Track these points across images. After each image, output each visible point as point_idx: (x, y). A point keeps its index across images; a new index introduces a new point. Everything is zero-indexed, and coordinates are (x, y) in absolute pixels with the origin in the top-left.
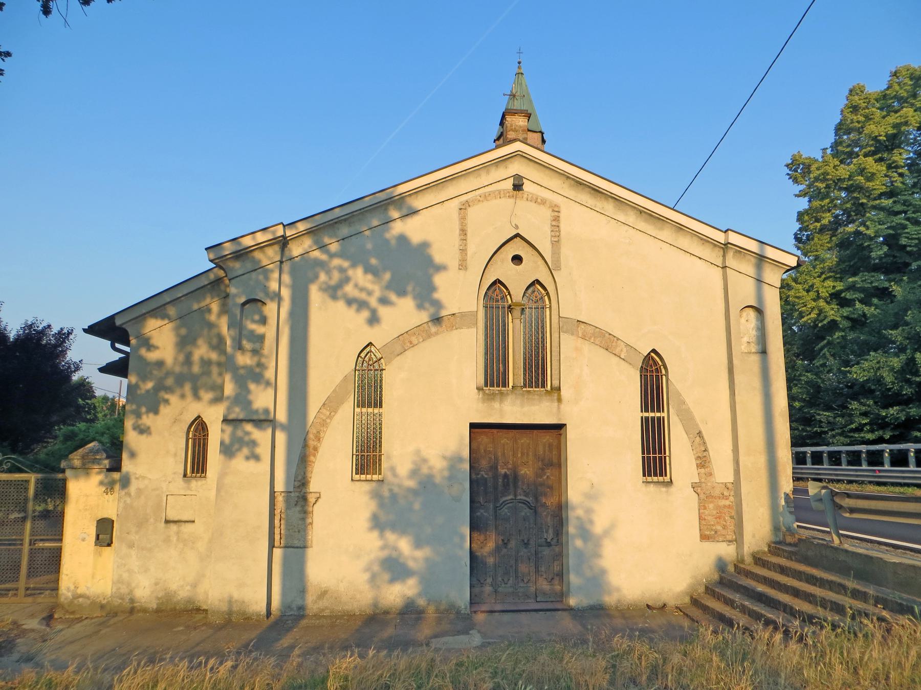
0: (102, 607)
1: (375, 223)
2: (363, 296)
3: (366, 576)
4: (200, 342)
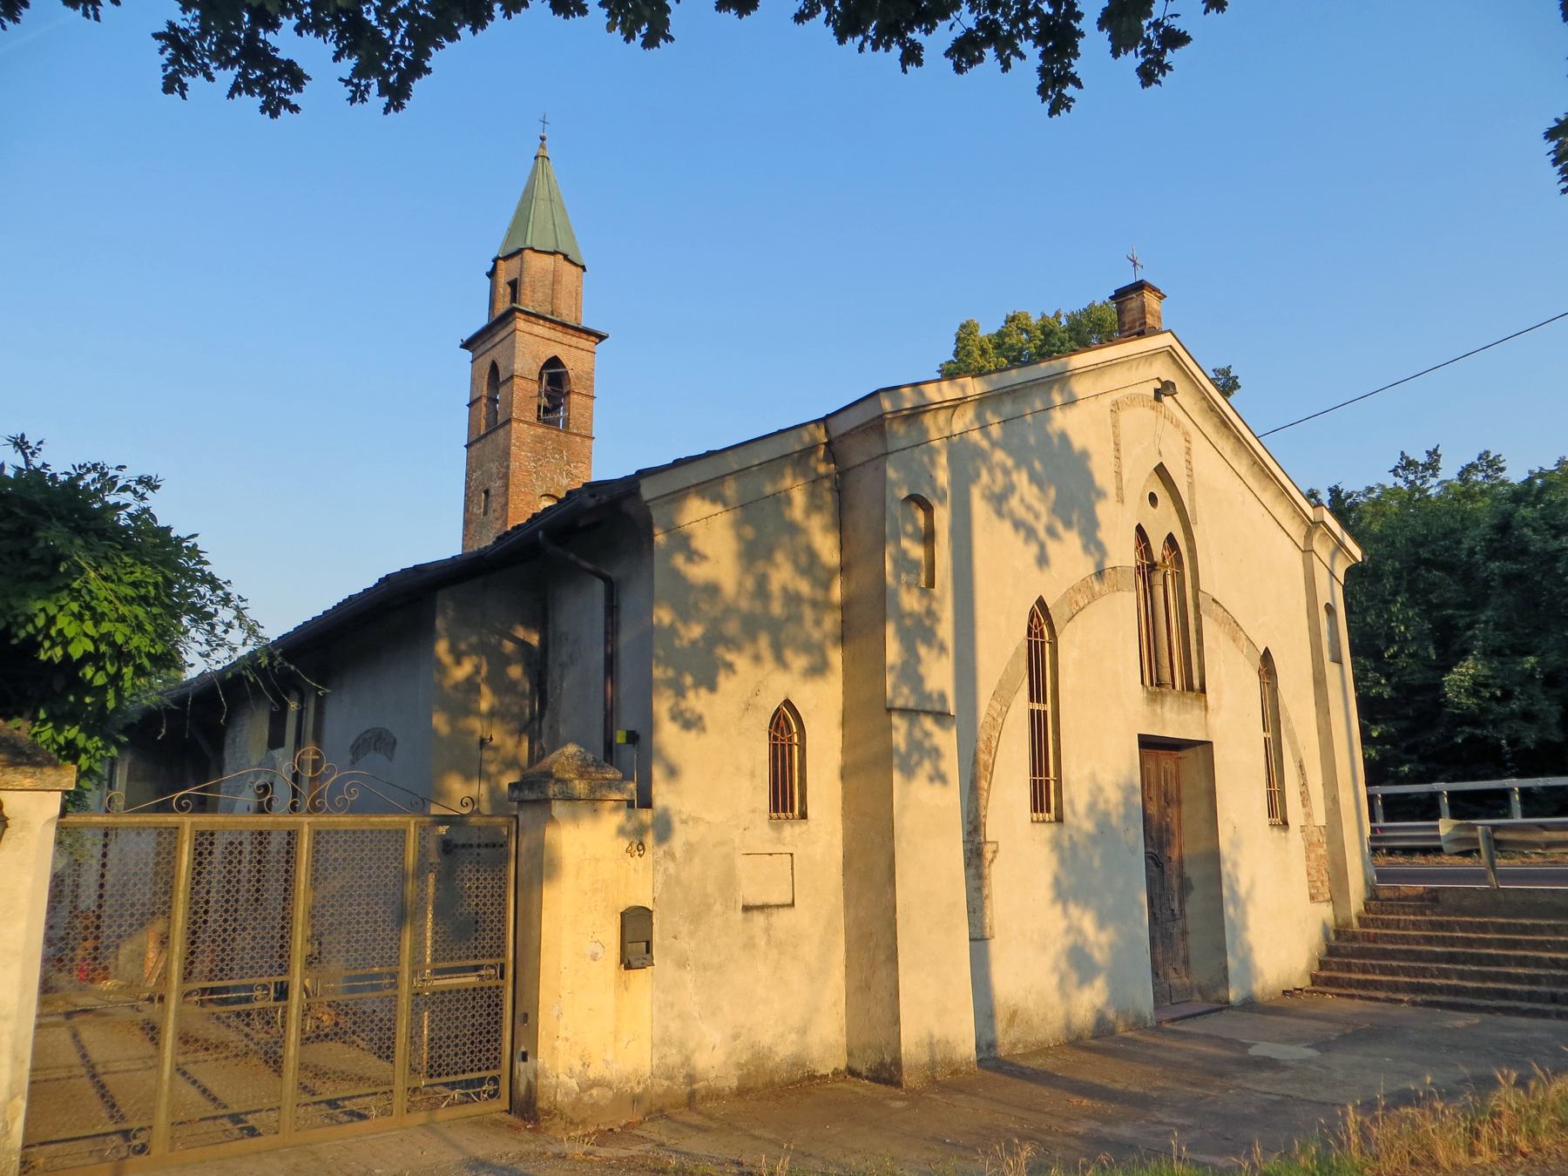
0: (636, 1100)
1: (1038, 405)
2: (1030, 518)
3: (1054, 980)
4: (780, 557)
